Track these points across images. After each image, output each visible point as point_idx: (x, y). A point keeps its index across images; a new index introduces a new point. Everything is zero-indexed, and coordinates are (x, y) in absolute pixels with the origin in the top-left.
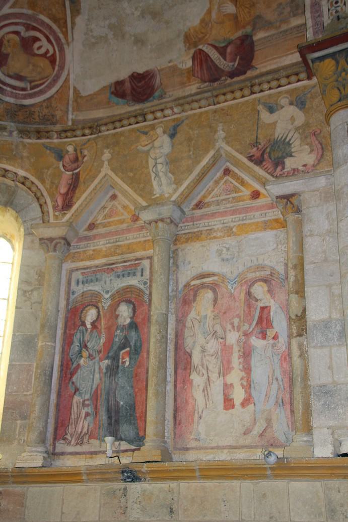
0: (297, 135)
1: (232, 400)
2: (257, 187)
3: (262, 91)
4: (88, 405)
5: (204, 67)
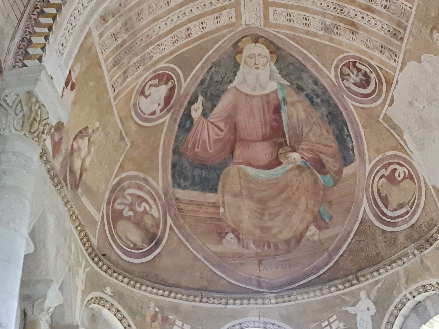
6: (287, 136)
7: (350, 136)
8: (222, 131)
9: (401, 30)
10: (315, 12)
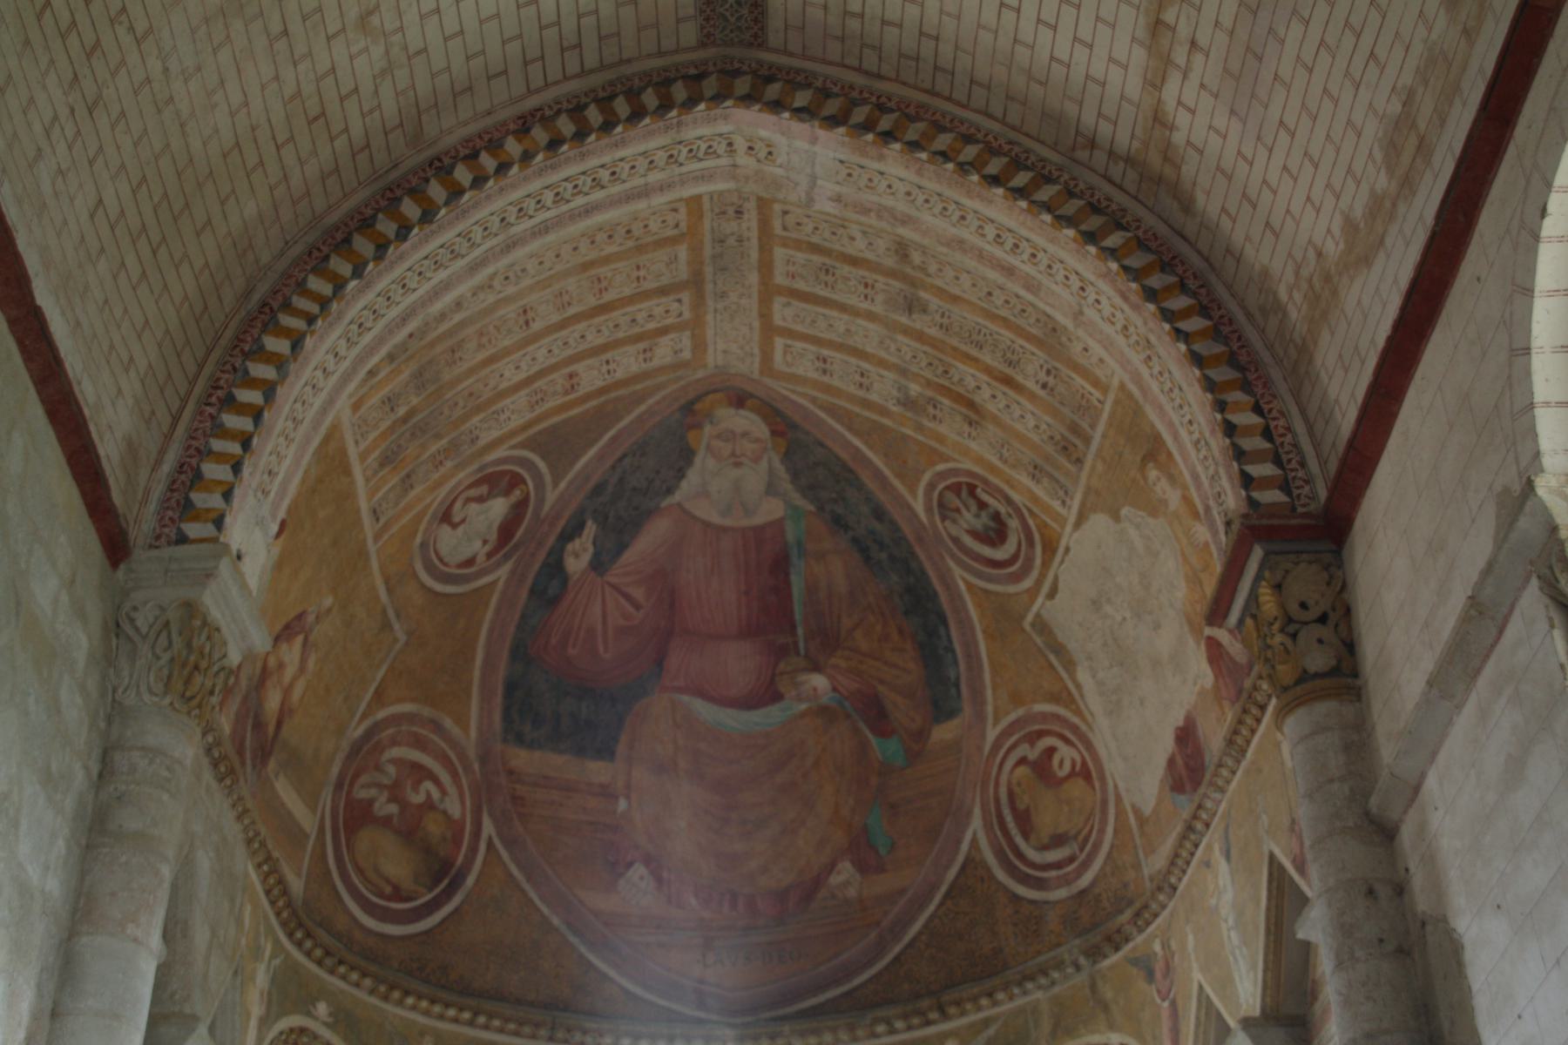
6: (800, 631)
7: (953, 651)
8: (638, 607)
9: (1078, 442)
10: (882, 363)
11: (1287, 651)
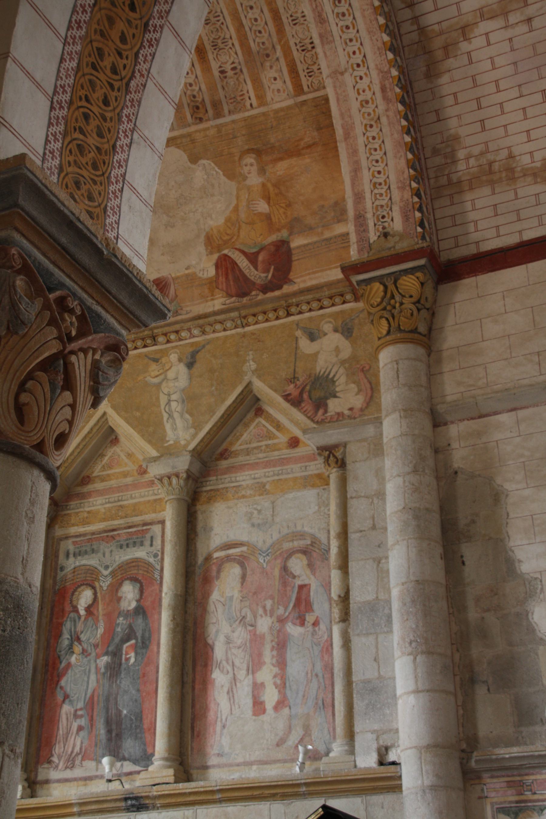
0: (342, 371)
1: (262, 703)
2: (298, 433)
3: (300, 313)
4: (81, 716)
5: (230, 277)
11: (412, 315)
